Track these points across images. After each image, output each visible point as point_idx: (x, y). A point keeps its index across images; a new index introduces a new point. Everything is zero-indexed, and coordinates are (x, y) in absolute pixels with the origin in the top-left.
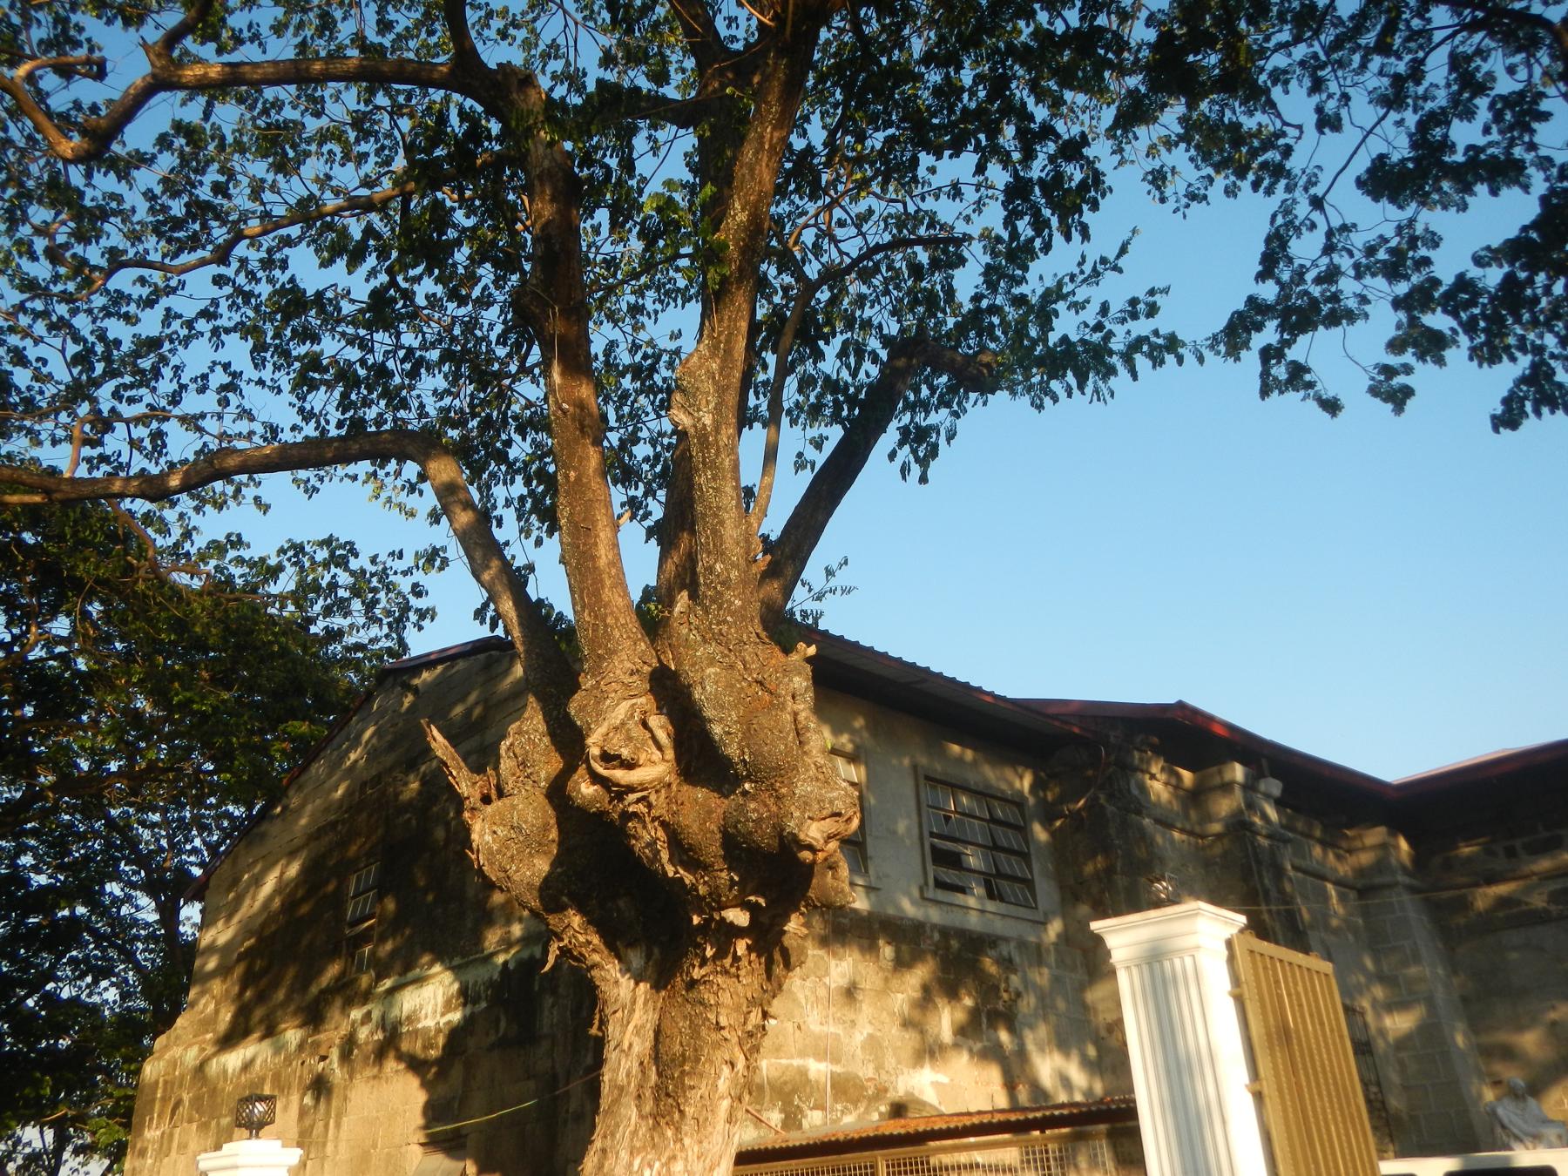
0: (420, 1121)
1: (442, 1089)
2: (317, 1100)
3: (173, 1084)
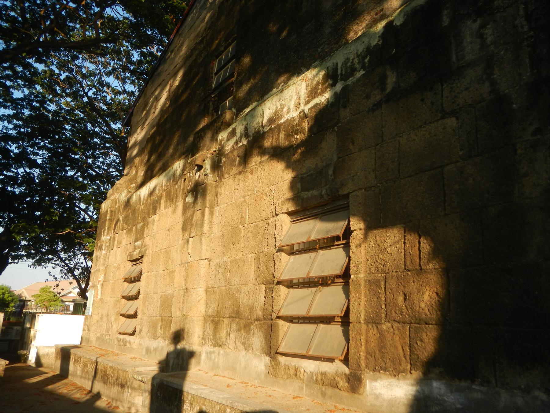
0: (288, 194)
1: (311, 163)
3: (115, 212)
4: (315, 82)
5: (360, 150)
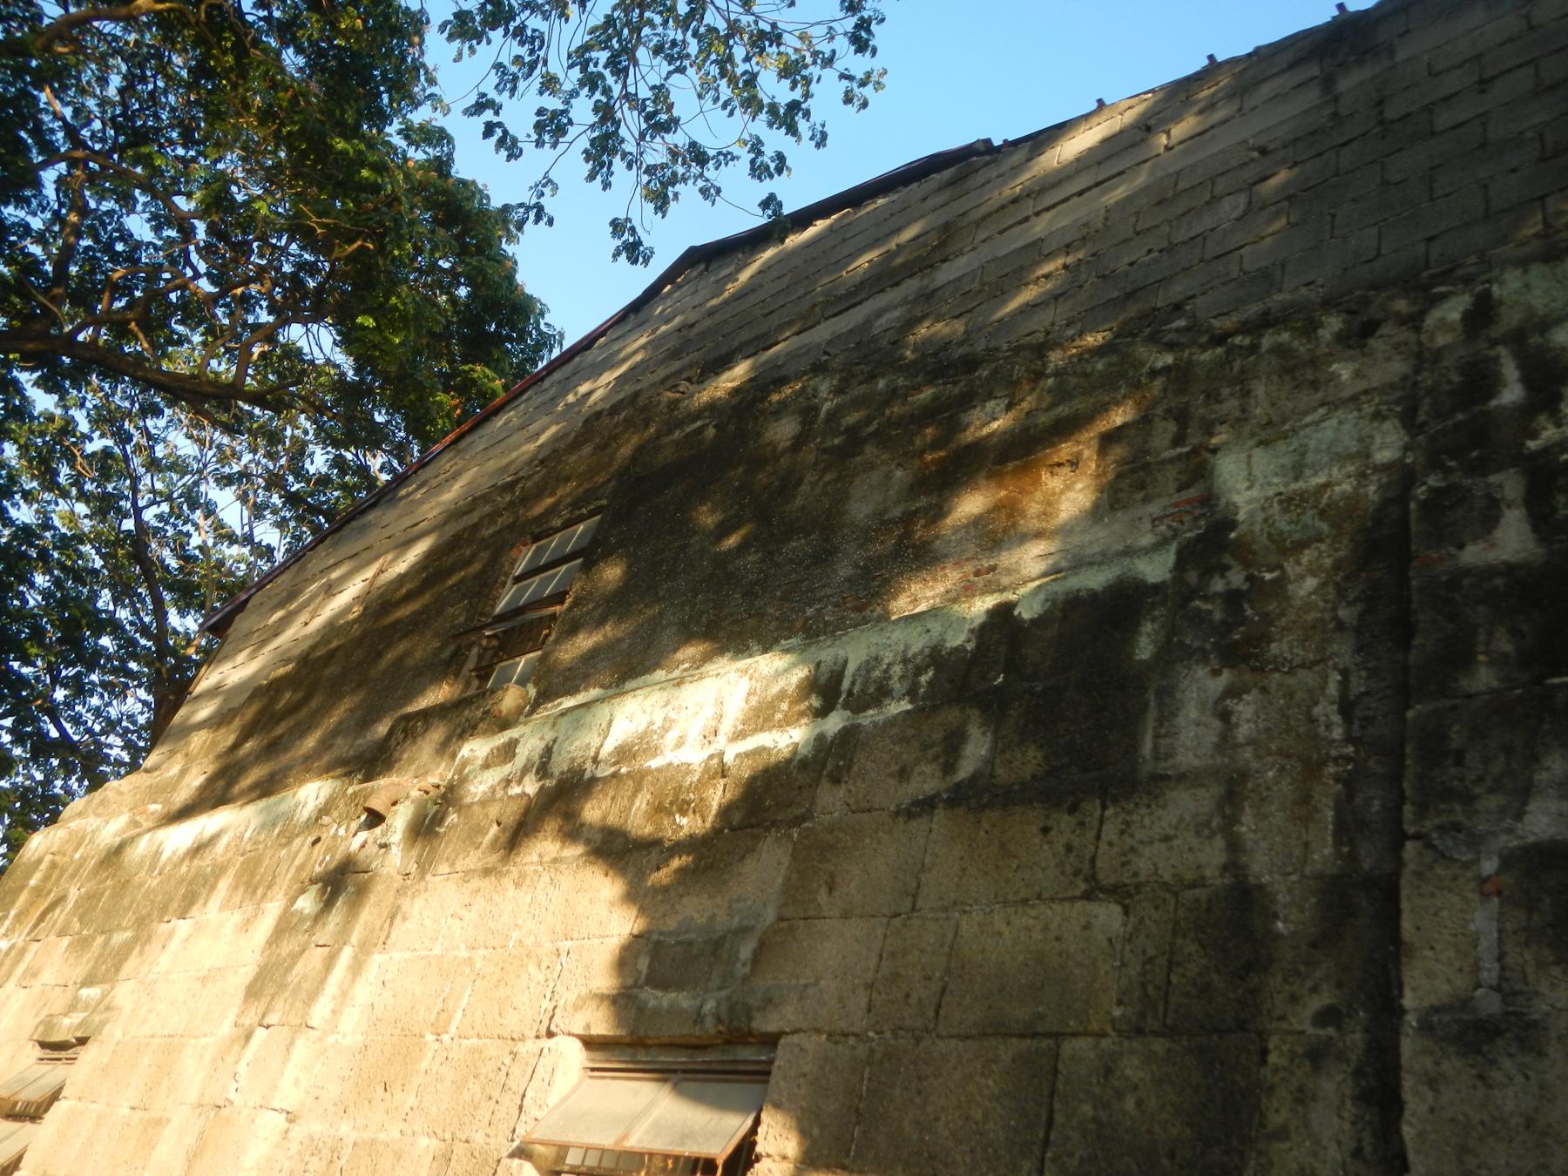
0: (604, 981)
2: (328, 904)
4: (775, 689)
5: (846, 915)
